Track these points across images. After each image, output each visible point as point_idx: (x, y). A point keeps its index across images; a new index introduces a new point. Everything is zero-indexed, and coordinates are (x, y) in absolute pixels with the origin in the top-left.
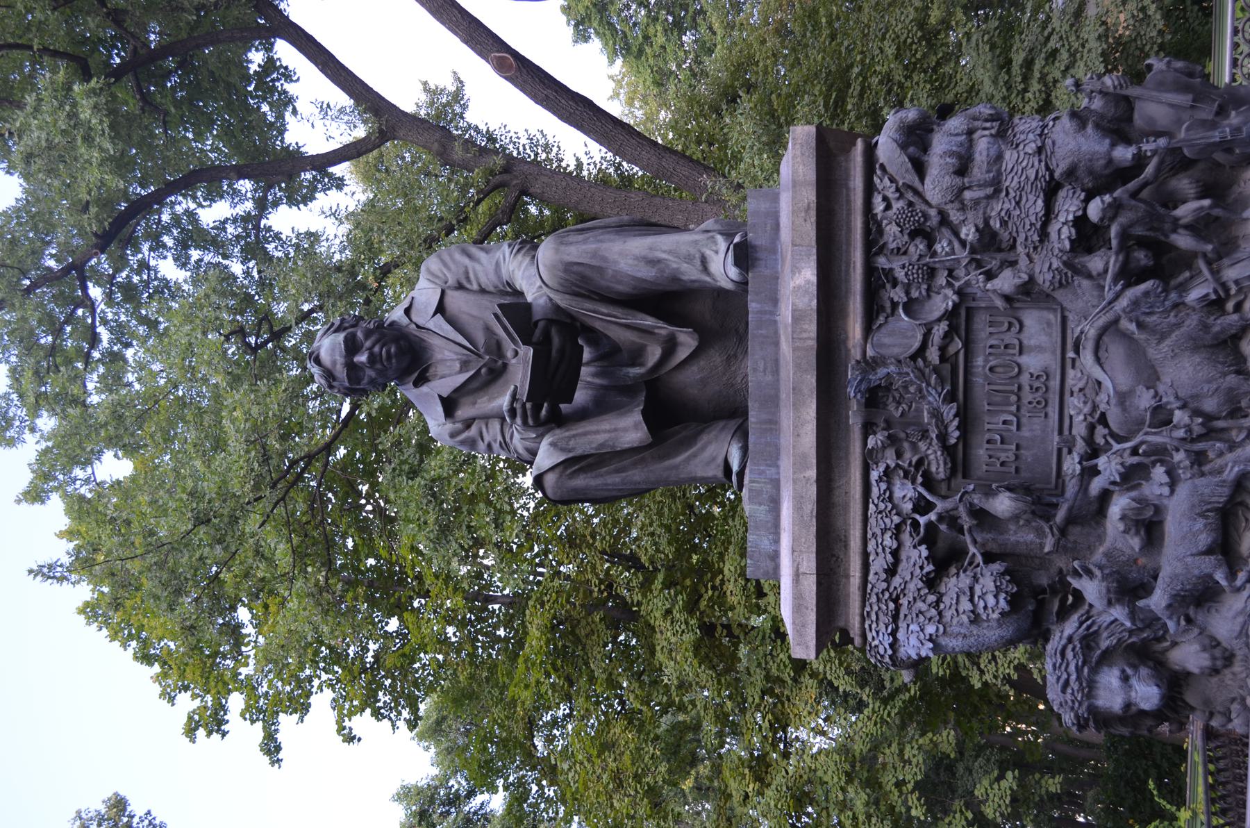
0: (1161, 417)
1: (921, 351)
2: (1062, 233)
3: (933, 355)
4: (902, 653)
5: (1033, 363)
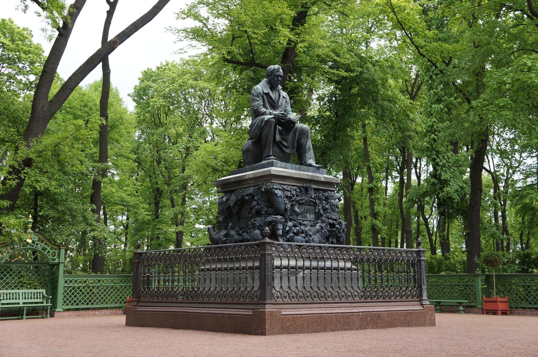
0: (310, 236)
1: (312, 198)
2: (331, 221)
3: (311, 199)
4: (274, 190)
5: (308, 215)
